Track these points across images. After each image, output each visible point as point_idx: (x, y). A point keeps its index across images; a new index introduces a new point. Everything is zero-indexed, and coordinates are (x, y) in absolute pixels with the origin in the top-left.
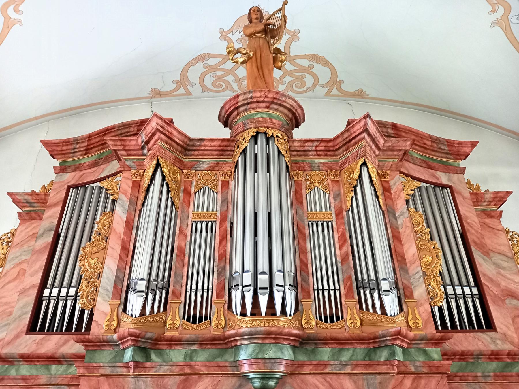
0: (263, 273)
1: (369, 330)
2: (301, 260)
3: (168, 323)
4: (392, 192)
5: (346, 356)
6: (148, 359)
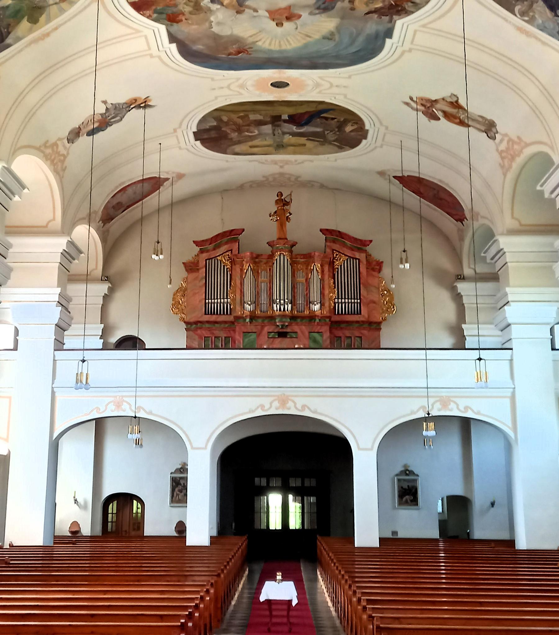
0: (282, 300)
1: (311, 315)
2: (294, 295)
3: (256, 313)
4: (325, 272)
5: (304, 321)
6: (252, 321)
